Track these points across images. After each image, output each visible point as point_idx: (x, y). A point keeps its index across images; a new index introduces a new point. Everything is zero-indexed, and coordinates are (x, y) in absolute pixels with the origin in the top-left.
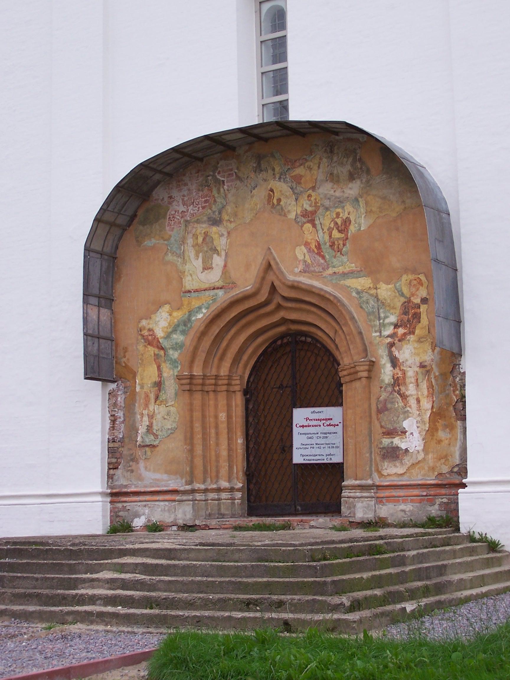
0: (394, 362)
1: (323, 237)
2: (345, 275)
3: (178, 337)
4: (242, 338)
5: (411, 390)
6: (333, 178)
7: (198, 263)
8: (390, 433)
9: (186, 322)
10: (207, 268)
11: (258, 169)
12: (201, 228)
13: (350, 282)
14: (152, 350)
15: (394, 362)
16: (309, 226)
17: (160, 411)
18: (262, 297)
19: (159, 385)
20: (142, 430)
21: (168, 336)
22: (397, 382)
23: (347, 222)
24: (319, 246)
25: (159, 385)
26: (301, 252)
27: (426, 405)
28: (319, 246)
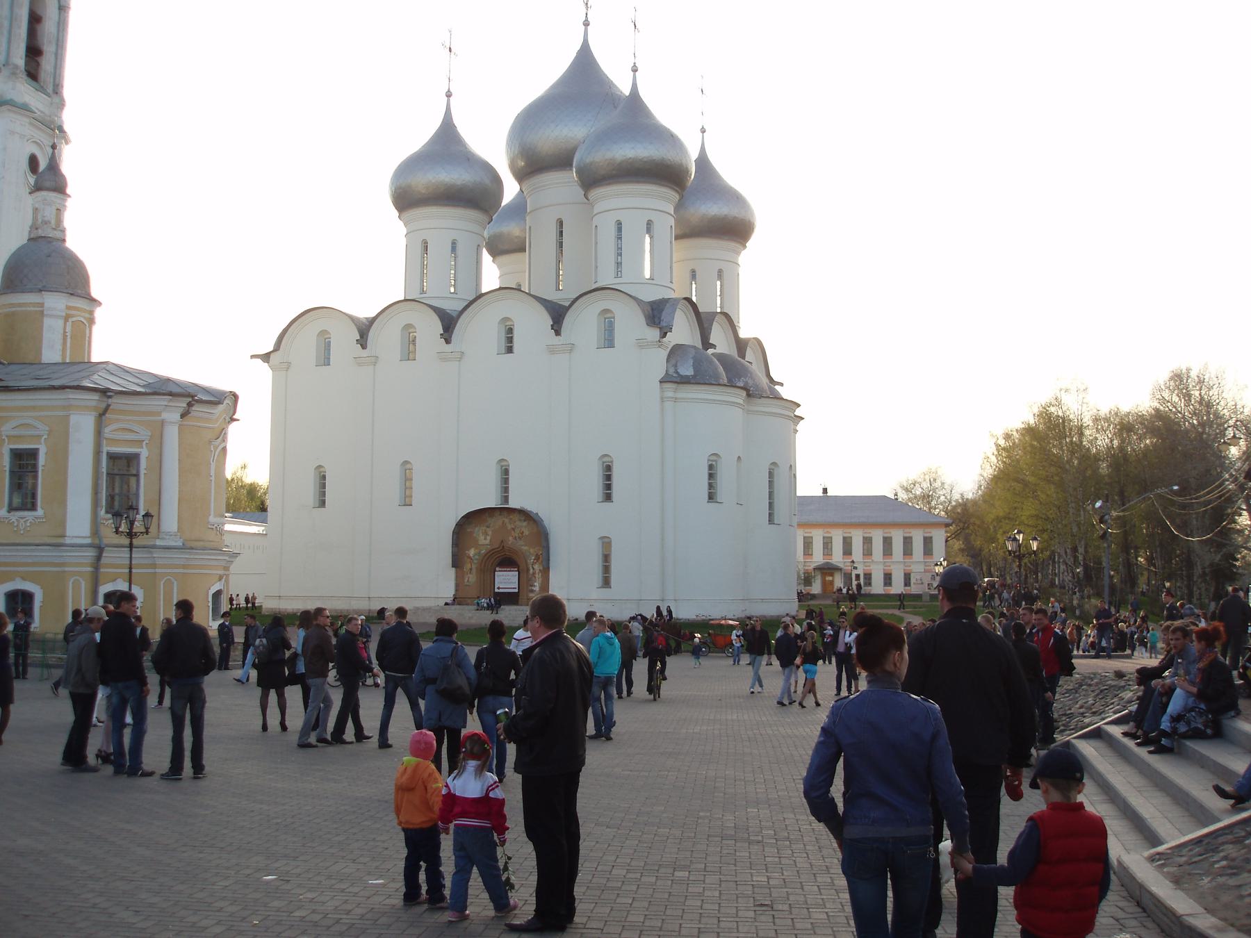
0: (533, 569)
1: (517, 535)
2: (522, 546)
3: (477, 557)
4: (493, 560)
5: (537, 576)
6: (520, 520)
7: (482, 538)
8: (532, 586)
9: (480, 553)
10: (485, 539)
11: (500, 515)
12: (484, 528)
13: (523, 547)
14: (469, 560)
15: (533, 569)
16: (513, 532)
17: (471, 576)
18: (501, 548)
19: (471, 569)
20: (466, 580)
21: (474, 556)
22: (534, 573)
23: (523, 532)
24: (515, 537)
25: (471, 569)
26: (511, 538)
27: (540, 579)
28: (515, 537)
